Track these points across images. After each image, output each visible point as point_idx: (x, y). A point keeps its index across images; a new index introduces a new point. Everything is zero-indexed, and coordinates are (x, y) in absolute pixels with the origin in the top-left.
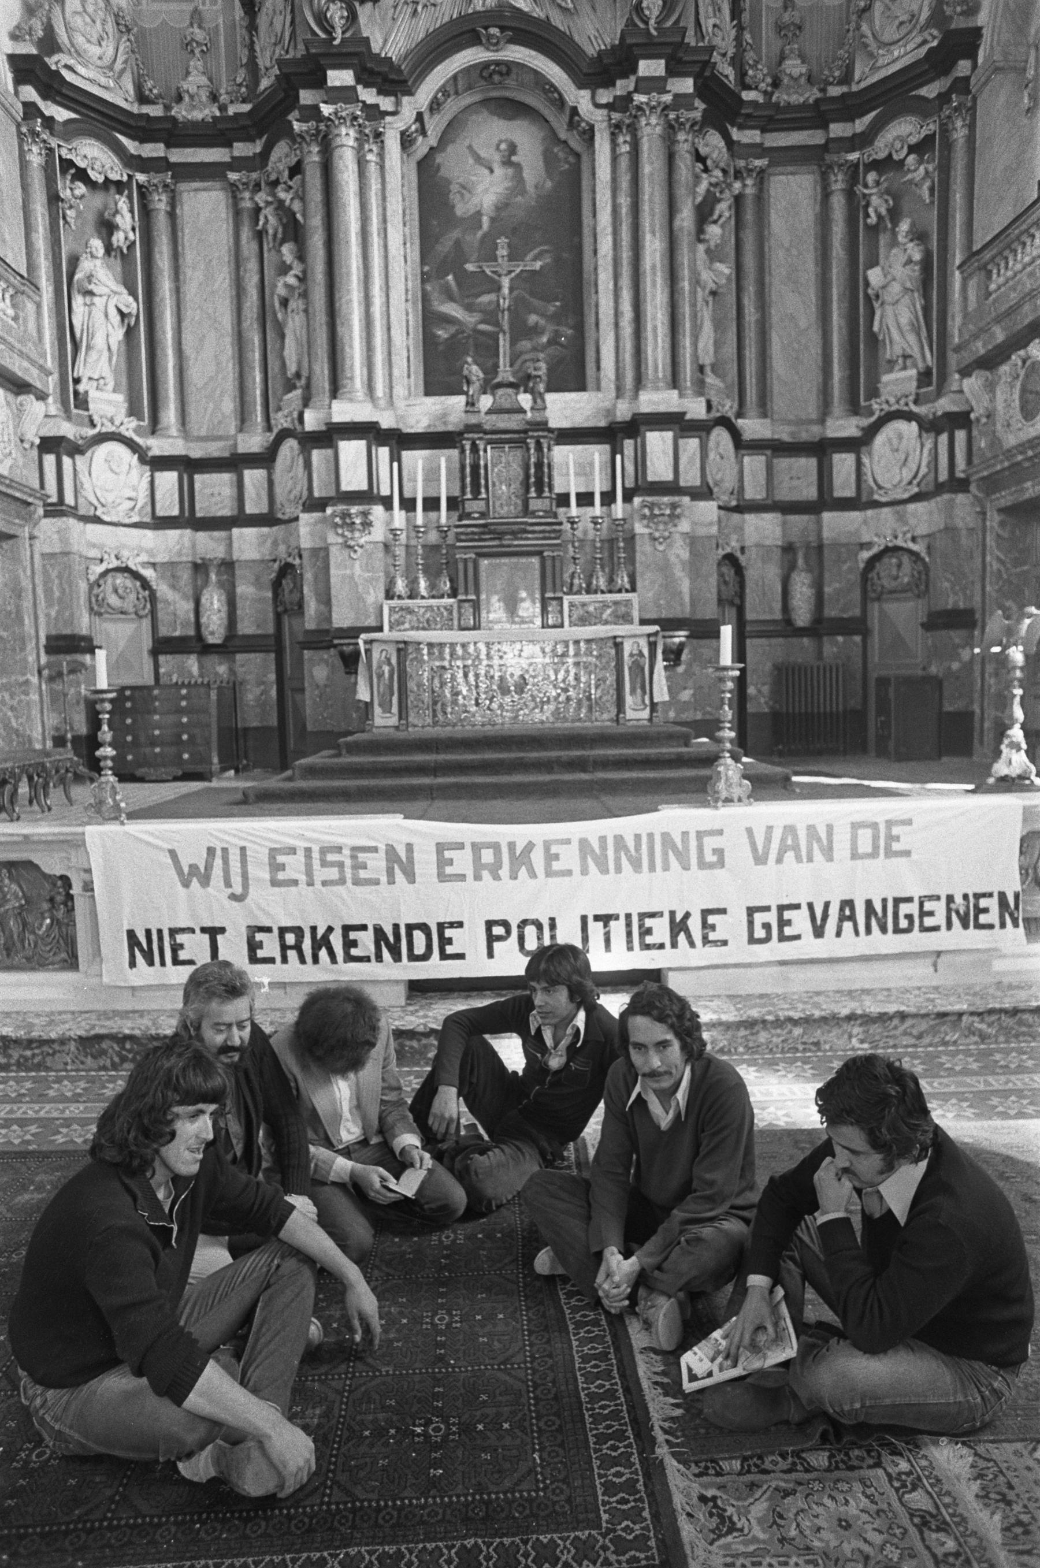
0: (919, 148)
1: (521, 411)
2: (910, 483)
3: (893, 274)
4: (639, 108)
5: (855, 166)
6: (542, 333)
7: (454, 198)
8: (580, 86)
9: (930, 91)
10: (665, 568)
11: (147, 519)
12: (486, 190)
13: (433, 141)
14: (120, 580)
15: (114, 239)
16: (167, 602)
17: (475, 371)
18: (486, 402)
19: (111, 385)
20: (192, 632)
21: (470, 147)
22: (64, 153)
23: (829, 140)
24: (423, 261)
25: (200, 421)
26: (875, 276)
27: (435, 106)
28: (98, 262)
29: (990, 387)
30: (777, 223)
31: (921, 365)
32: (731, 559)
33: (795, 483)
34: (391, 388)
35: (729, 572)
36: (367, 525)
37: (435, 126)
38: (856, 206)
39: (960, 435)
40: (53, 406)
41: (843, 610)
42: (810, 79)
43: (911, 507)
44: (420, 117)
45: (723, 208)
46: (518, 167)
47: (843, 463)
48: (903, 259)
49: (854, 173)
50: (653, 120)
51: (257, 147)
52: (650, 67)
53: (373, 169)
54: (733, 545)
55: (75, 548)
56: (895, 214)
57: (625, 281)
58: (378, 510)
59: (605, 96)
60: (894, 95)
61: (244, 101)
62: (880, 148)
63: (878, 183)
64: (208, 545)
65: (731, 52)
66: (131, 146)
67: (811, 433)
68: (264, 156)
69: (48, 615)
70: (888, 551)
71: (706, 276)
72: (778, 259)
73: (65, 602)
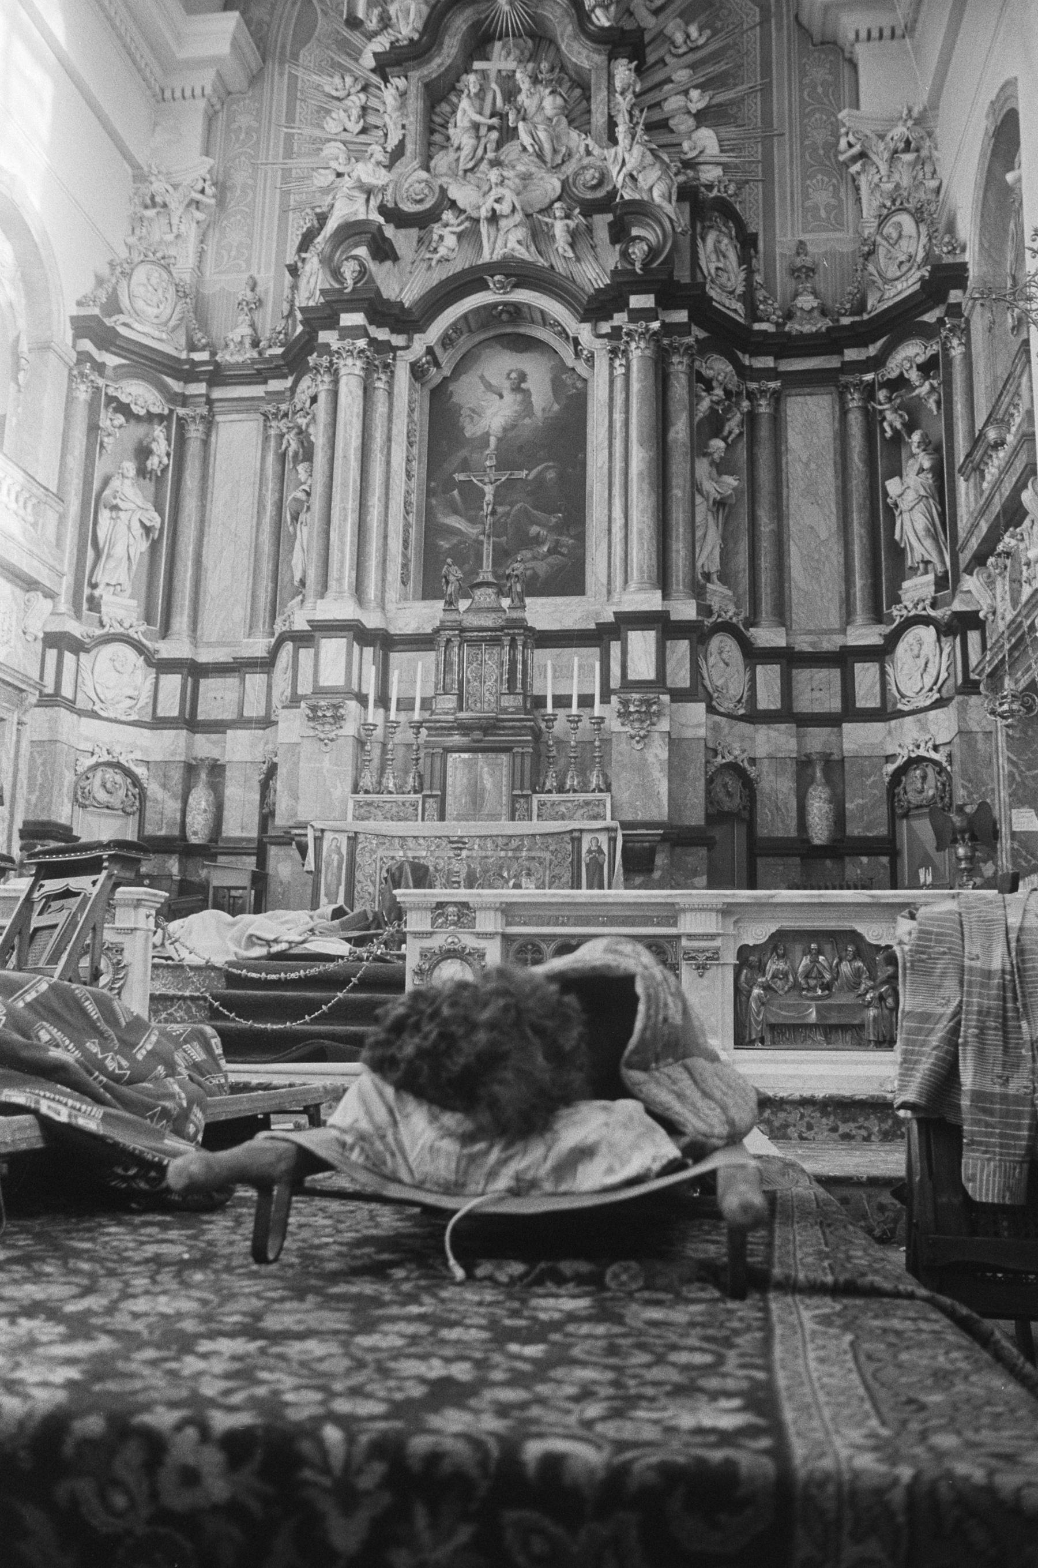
0: (927, 368)
5: (871, 385)
6: (543, 543)
7: (465, 422)
8: (583, 321)
10: (641, 768)
11: (148, 719)
12: (495, 414)
14: (110, 775)
15: (149, 463)
16: (156, 801)
19: (129, 591)
20: (176, 833)
21: (482, 377)
22: (111, 391)
23: (843, 363)
24: (429, 478)
26: (893, 486)
27: (446, 341)
28: (128, 482)
29: (990, 583)
30: (794, 439)
31: (940, 569)
32: (735, 768)
33: (817, 694)
34: (383, 592)
35: (733, 783)
37: (447, 360)
38: (872, 420)
39: (973, 637)
40: (64, 605)
41: (868, 828)
43: (932, 713)
44: (430, 351)
45: (733, 425)
46: (527, 393)
47: (866, 674)
48: (916, 467)
49: (869, 392)
50: (642, 344)
51: (289, 382)
52: (638, 301)
54: (736, 752)
55: (63, 738)
56: (911, 427)
57: (617, 490)
58: (353, 705)
59: (605, 328)
60: (900, 322)
62: (894, 367)
63: (890, 400)
65: (740, 290)
66: (176, 386)
67: (831, 644)
68: (293, 390)
69: (28, 801)
71: (708, 486)
73: (45, 789)
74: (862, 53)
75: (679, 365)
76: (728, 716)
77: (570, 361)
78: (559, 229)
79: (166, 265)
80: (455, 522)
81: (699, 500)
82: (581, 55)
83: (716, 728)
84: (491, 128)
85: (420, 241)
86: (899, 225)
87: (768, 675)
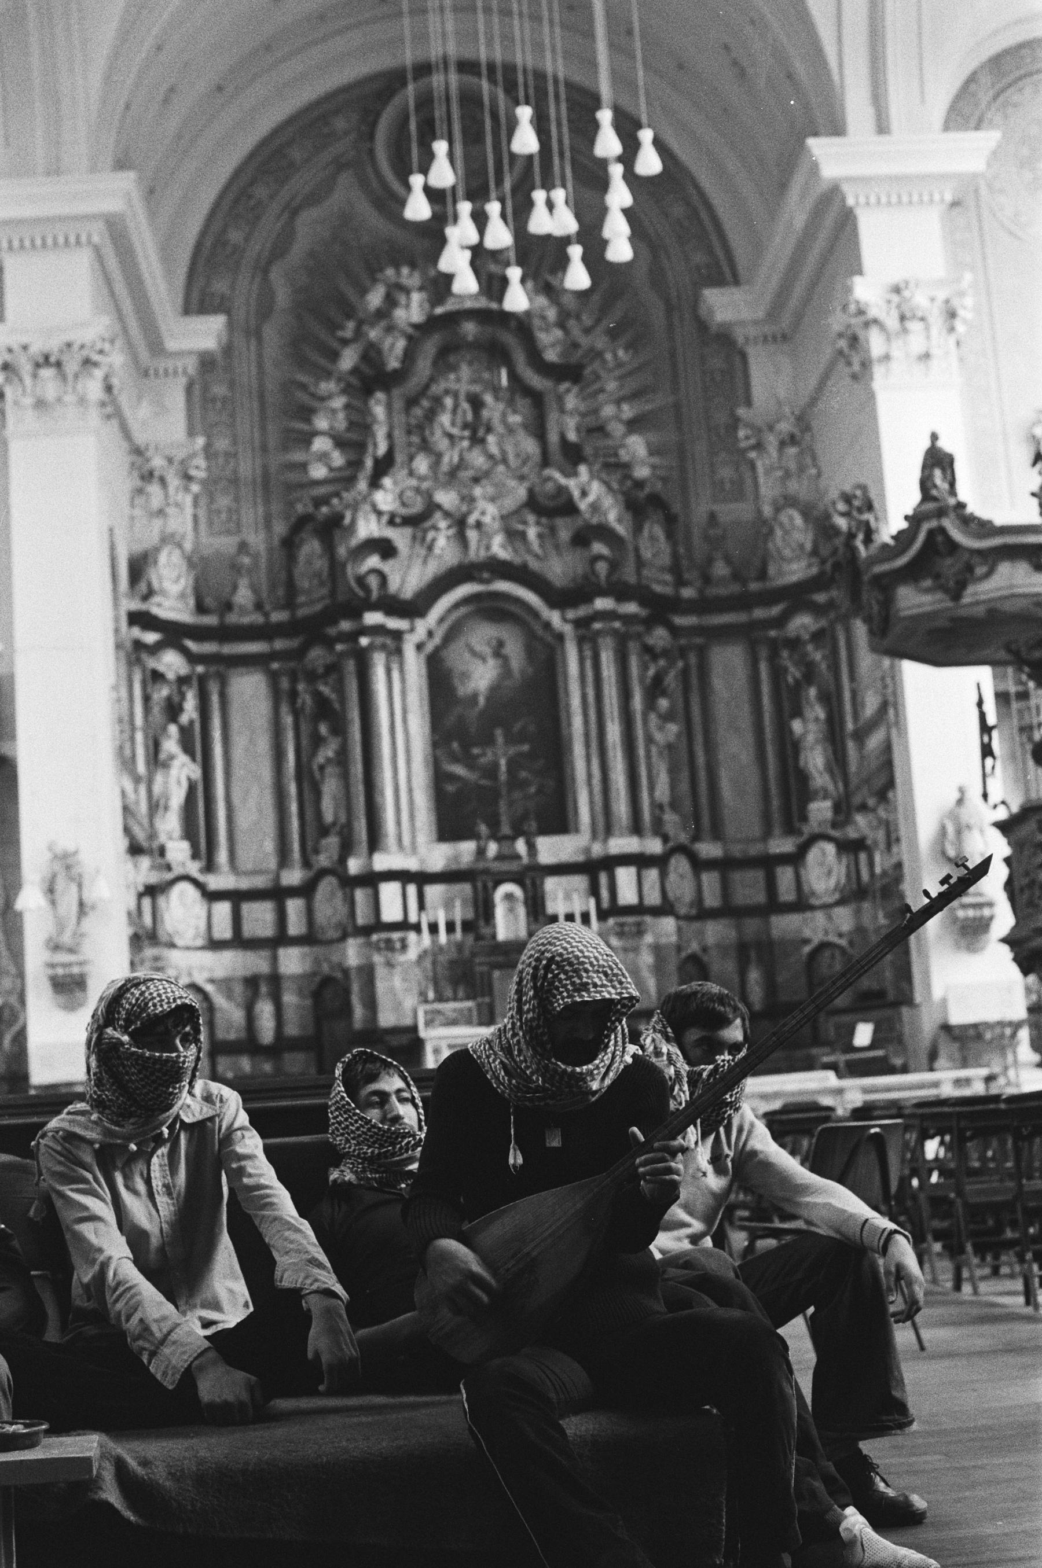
0: (818, 637)
1: (518, 857)
3: (810, 727)
4: (598, 633)
7: (456, 682)
9: (821, 598)
13: (437, 640)
16: (221, 1009)
17: (483, 829)
18: (493, 848)
25: (247, 858)
27: (441, 620)
30: (718, 683)
32: (693, 958)
36: (404, 947)
42: (736, 576)
44: (430, 634)
45: (671, 680)
47: (785, 876)
49: (775, 648)
52: (602, 604)
53: (396, 675)
54: (694, 947)
59: (571, 614)
61: (283, 608)
64: (257, 962)
66: (191, 645)
67: (755, 850)
68: (300, 653)
70: (823, 946)
71: (658, 737)
72: (721, 711)
74: (751, 351)
75: (633, 646)
76: (688, 918)
77: (540, 632)
78: (532, 533)
79: (180, 546)
80: (459, 770)
81: (654, 750)
82: (535, 381)
83: (679, 930)
84: (462, 438)
85: (414, 538)
86: (791, 519)
87: (710, 880)
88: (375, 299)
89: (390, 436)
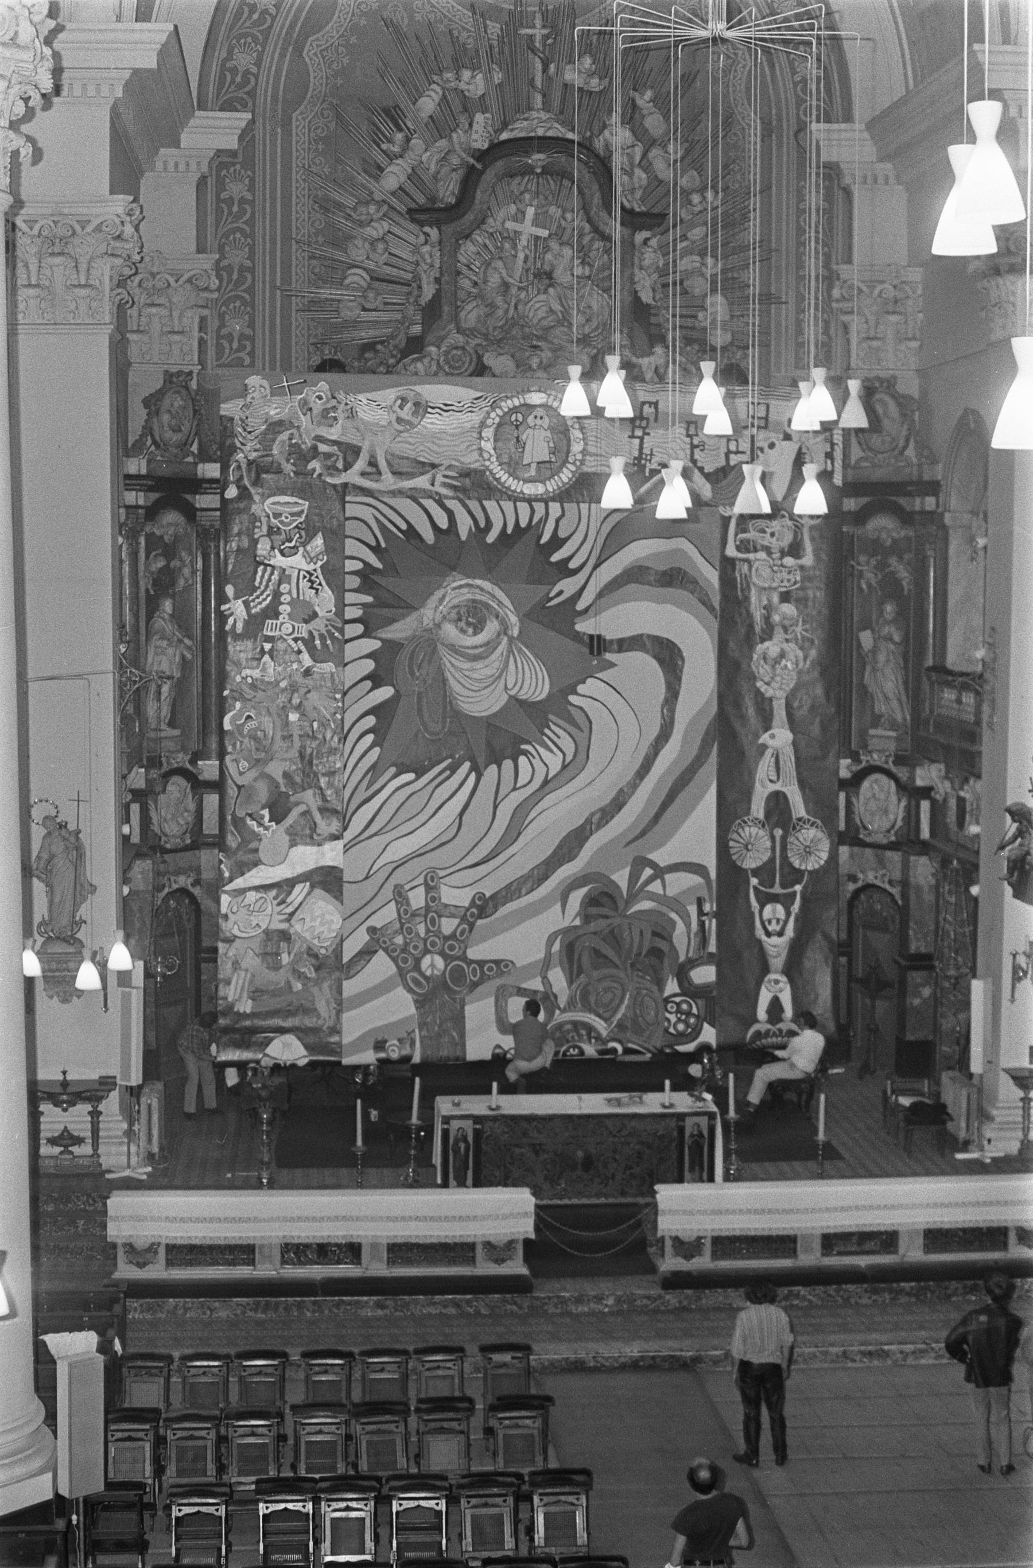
2: (888, 831)
43: (889, 854)
63: (868, 563)
88: (428, 104)
89: (437, 280)
